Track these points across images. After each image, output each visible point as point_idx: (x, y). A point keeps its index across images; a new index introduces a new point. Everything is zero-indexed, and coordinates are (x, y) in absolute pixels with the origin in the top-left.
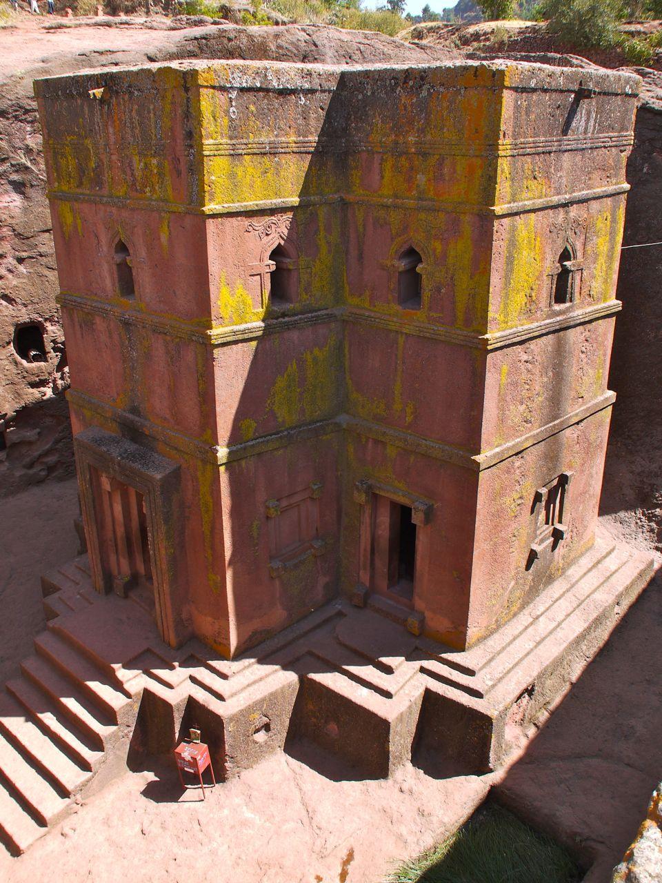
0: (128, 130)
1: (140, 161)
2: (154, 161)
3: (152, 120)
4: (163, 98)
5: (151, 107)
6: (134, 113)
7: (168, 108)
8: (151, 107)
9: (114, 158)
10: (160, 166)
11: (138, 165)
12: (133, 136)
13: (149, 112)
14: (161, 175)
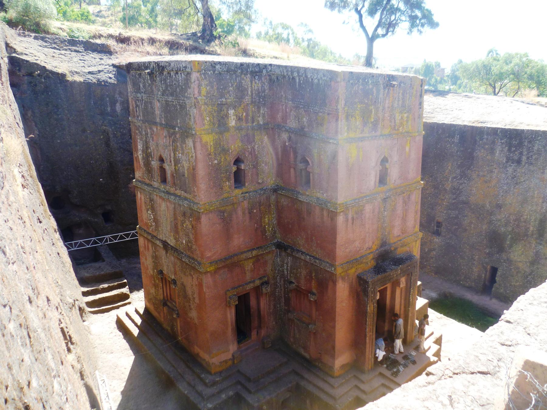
0: (396, 102)
1: (399, 116)
2: (405, 115)
3: (408, 98)
4: (413, 88)
5: (408, 92)
6: (400, 94)
7: (415, 93)
8: (408, 92)
9: (386, 115)
10: (408, 117)
11: (398, 117)
12: (398, 104)
13: (407, 94)
14: (407, 121)
